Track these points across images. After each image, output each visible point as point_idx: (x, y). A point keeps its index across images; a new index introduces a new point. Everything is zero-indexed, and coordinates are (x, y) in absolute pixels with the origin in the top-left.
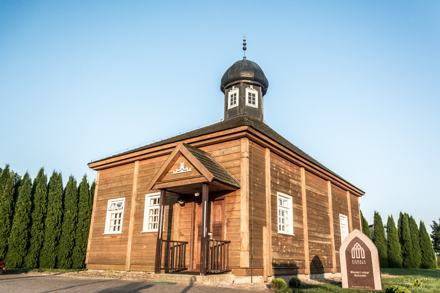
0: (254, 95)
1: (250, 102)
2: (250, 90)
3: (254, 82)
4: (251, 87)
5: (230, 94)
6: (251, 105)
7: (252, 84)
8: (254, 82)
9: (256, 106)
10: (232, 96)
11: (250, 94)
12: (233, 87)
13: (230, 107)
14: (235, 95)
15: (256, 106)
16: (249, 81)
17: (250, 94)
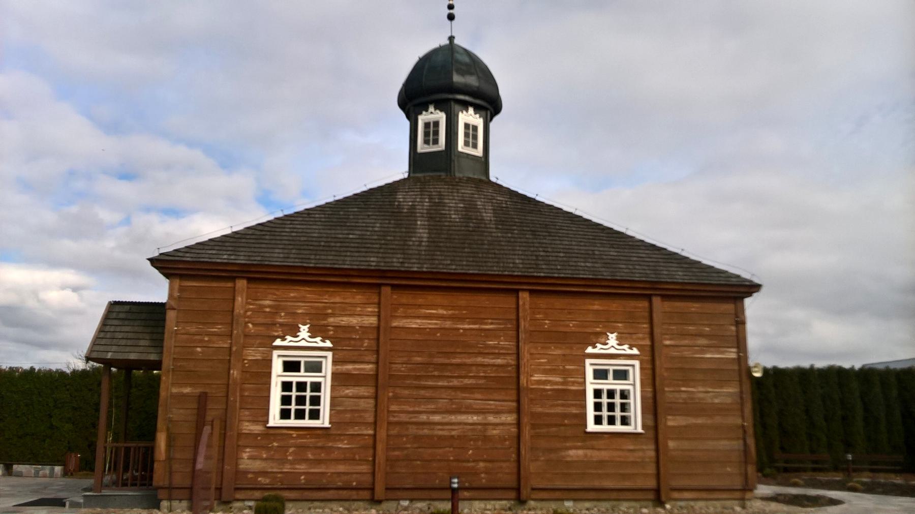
0: (475, 128)
1: (466, 144)
2: (468, 117)
3: (478, 102)
4: (471, 110)
5: (422, 119)
6: (470, 151)
7: (472, 104)
8: (478, 102)
9: (479, 152)
10: (427, 125)
11: (467, 126)
12: (431, 109)
13: (421, 148)
14: (436, 124)
15: (479, 152)
16: (467, 98)
17: (467, 126)
